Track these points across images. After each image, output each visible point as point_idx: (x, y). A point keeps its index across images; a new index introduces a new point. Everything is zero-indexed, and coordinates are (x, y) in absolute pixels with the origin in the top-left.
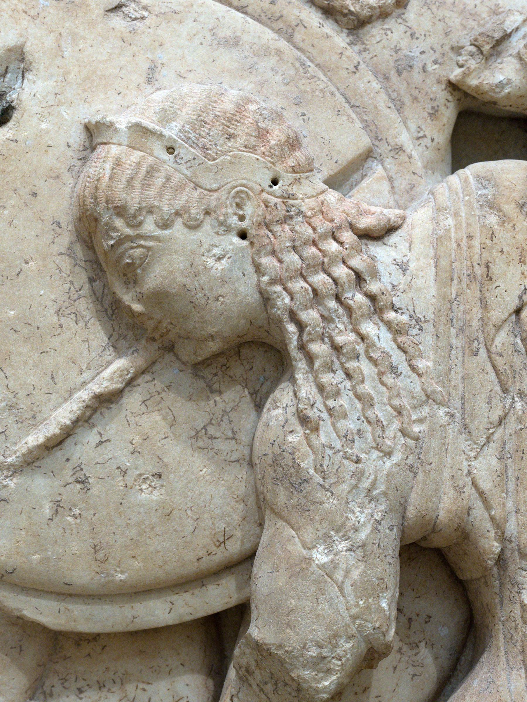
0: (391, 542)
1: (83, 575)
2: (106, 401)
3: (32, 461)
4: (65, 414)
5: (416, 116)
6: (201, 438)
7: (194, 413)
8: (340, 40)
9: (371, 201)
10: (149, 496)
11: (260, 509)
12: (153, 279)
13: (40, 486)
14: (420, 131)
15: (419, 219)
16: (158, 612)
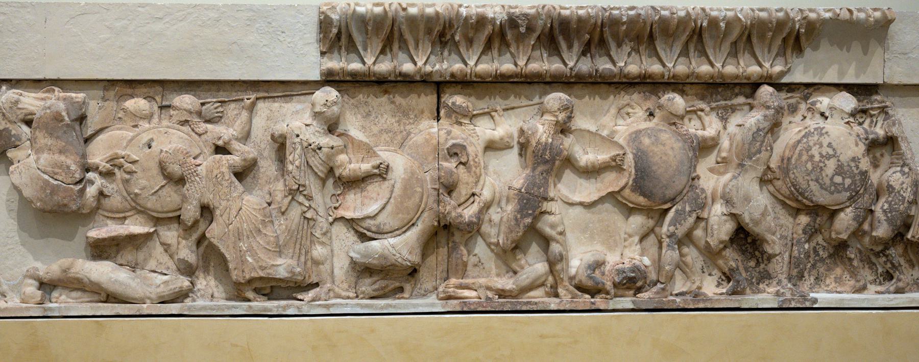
0: (199, 206)
1: (160, 210)
2: (163, 186)
3: (153, 194)
4: (157, 188)
5: (208, 148)
6: (175, 192)
7: (174, 188)
8: (197, 137)
9: (198, 161)
10: (169, 199)
11: (183, 201)
12: (168, 171)
13: (154, 197)
14: (208, 150)
15: (205, 163)
16: (170, 215)
